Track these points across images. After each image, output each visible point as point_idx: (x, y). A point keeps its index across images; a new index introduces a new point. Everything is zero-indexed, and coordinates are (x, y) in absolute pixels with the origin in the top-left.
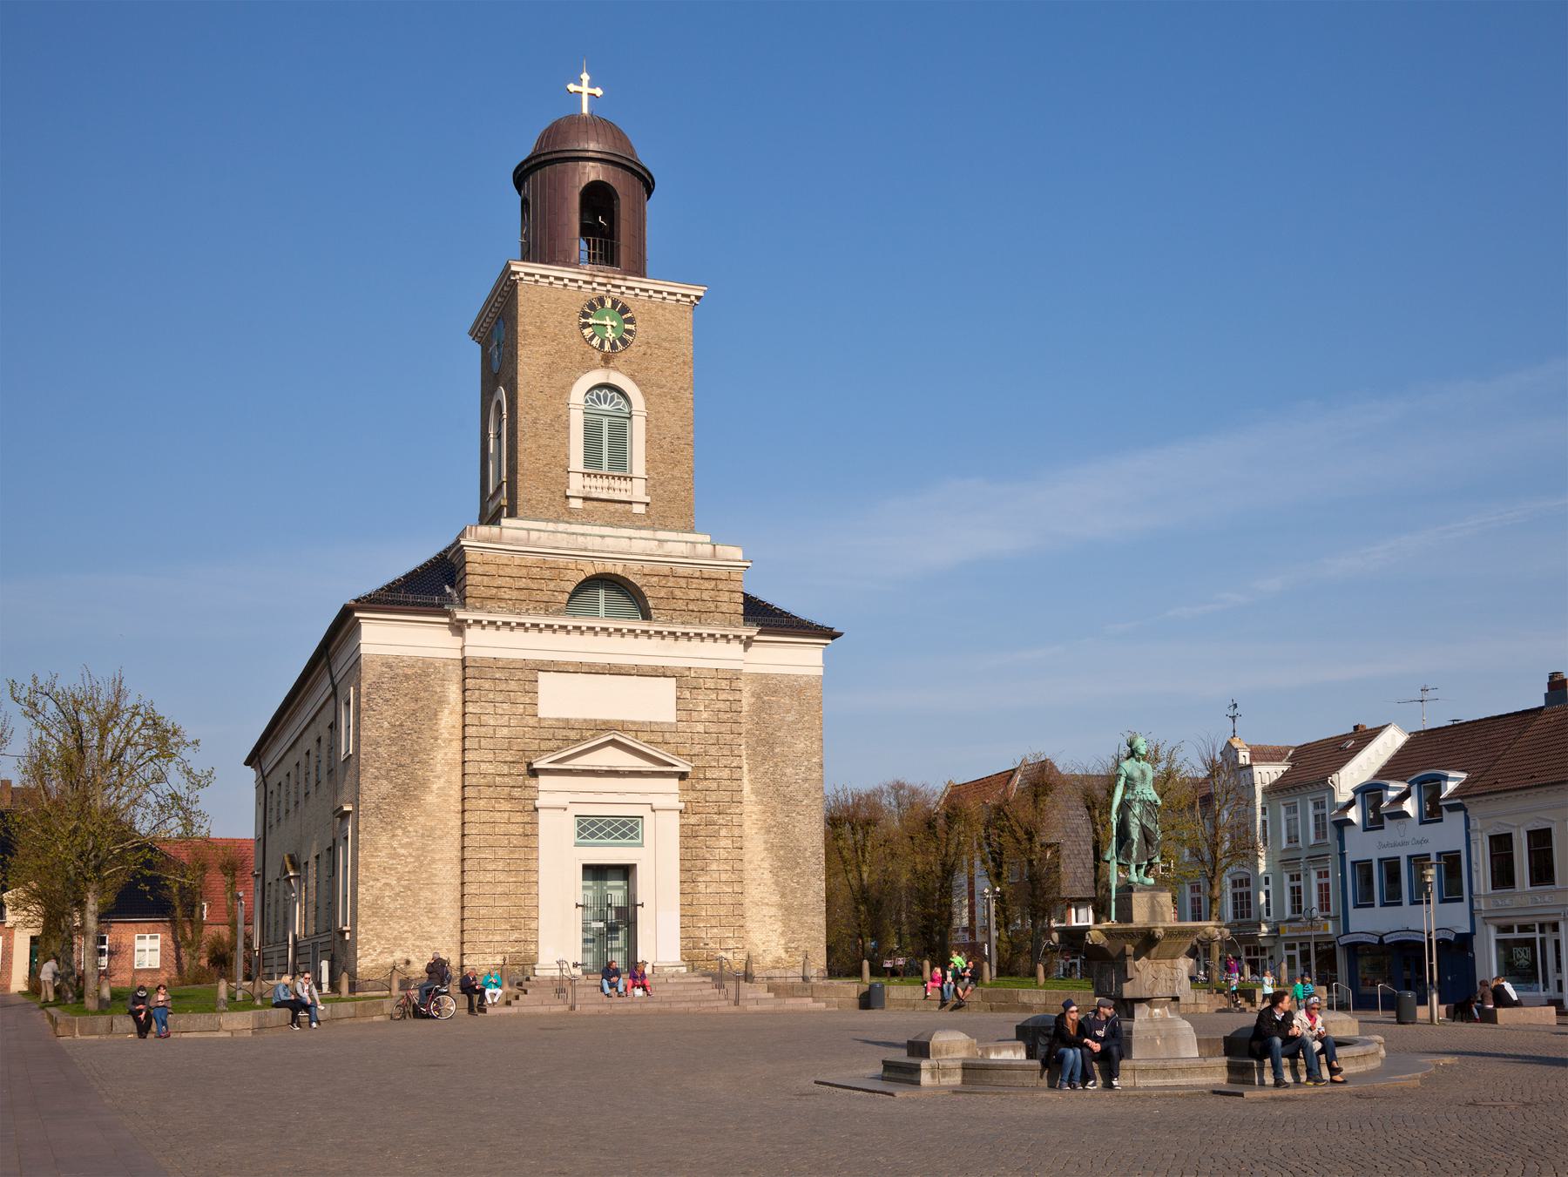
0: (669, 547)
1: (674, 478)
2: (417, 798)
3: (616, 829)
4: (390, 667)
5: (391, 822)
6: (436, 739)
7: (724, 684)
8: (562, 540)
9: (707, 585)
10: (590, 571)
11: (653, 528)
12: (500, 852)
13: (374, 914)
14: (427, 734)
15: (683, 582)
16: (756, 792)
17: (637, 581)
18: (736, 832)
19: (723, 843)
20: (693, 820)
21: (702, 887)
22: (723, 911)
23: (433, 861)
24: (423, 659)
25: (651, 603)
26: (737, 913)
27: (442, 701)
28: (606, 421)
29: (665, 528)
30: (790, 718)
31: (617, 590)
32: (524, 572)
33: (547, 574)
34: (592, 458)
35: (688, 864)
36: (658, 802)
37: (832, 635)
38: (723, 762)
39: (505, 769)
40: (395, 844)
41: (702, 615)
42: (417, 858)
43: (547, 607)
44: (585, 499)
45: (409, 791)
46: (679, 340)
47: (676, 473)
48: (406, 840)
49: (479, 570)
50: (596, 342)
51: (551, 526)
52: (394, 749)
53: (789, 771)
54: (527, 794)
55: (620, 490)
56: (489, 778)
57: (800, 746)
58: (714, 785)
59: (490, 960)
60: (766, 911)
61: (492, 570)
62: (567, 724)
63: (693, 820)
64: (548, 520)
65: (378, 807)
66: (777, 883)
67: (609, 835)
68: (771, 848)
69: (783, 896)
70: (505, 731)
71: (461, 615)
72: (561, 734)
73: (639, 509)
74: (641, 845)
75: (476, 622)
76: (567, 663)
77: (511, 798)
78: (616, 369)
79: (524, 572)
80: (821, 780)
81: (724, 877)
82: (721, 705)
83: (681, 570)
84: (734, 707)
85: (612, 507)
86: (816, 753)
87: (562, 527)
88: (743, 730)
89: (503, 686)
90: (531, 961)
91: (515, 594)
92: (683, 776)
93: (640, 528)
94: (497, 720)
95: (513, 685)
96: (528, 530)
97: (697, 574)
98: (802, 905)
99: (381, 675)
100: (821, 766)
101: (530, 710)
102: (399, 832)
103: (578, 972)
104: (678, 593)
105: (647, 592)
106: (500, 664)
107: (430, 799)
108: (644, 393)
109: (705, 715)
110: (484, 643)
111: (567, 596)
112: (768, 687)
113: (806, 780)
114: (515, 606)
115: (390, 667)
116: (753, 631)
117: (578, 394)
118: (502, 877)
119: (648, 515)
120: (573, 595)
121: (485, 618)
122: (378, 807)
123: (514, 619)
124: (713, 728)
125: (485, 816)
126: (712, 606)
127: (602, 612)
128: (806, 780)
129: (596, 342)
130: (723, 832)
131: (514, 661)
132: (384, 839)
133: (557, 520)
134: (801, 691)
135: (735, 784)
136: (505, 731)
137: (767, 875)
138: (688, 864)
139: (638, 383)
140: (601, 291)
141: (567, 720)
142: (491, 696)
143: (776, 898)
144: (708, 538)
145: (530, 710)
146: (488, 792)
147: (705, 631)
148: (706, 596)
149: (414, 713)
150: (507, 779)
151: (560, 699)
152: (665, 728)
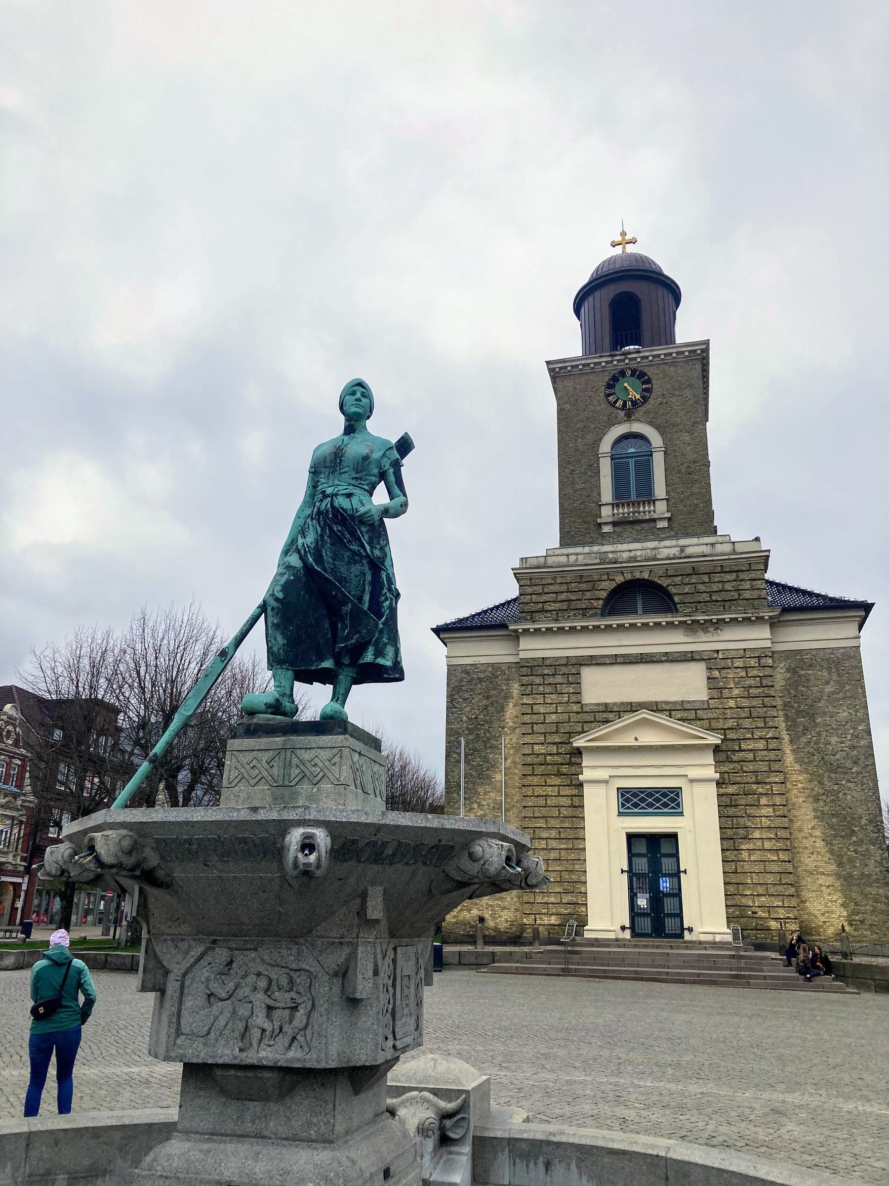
0: (689, 551)
1: (692, 494)
2: (489, 777)
3: (657, 800)
4: (468, 673)
6: (503, 728)
7: (753, 662)
9: (728, 577)
10: (620, 579)
11: (676, 537)
12: (553, 823)
14: (496, 725)
15: (706, 578)
16: (798, 761)
17: (664, 582)
18: (778, 800)
19: (765, 811)
20: (731, 789)
21: (745, 855)
22: (770, 879)
25: (676, 599)
26: (791, 884)
27: (507, 697)
28: (632, 462)
29: (686, 535)
30: (828, 689)
32: (564, 588)
33: (584, 586)
35: (729, 833)
36: (693, 773)
38: (758, 734)
39: (554, 749)
43: (584, 612)
50: (619, 404)
51: (587, 549)
52: (471, 737)
53: (834, 740)
54: (573, 769)
55: (645, 511)
57: (844, 715)
58: (750, 756)
59: (546, 920)
60: (822, 880)
61: (539, 589)
62: (607, 708)
63: (731, 789)
64: (583, 544)
66: (831, 852)
67: (650, 805)
68: (821, 816)
69: (840, 864)
73: (665, 524)
74: (681, 814)
75: (524, 630)
77: (559, 774)
79: (564, 588)
81: (767, 845)
82: (751, 682)
83: (702, 570)
84: (765, 682)
87: (596, 548)
88: (779, 702)
89: (551, 680)
90: (583, 922)
91: (557, 606)
92: (717, 749)
94: (549, 709)
95: (559, 679)
96: (568, 555)
97: (719, 569)
98: (863, 874)
99: (461, 680)
101: (573, 698)
102: (475, 806)
103: (627, 935)
104: (701, 588)
105: (673, 590)
106: (548, 662)
107: (499, 777)
109: (736, 692)
111: (601, 602)
113: (853, 748)
114: (557, 616)
115: (468, 673)
117: (606, 446)
118: (553, 844)
119: (670, 527)
120: (607, 600)
123: (554, 625)
124: (745, 703)
125: (539, 791)
126: (735, 595)
127: (640, 611)
128: (853, 748)
129: (619, 404)
130: (764, 801)
133: (593, 543)
134: (838, 663)
135: (772, 755)
136: (554, 717)
137: (820, 844)
138: (729, 833)
139: (658, 428)
140: (622, 366)
141: (606, 705)
142: (541, 688)
143: (833, 867)
145: (573, 698)
146: (540, 770)
148: (728, 586)
149: (486, 708)
150: (556, 758)
152: (698, 706)
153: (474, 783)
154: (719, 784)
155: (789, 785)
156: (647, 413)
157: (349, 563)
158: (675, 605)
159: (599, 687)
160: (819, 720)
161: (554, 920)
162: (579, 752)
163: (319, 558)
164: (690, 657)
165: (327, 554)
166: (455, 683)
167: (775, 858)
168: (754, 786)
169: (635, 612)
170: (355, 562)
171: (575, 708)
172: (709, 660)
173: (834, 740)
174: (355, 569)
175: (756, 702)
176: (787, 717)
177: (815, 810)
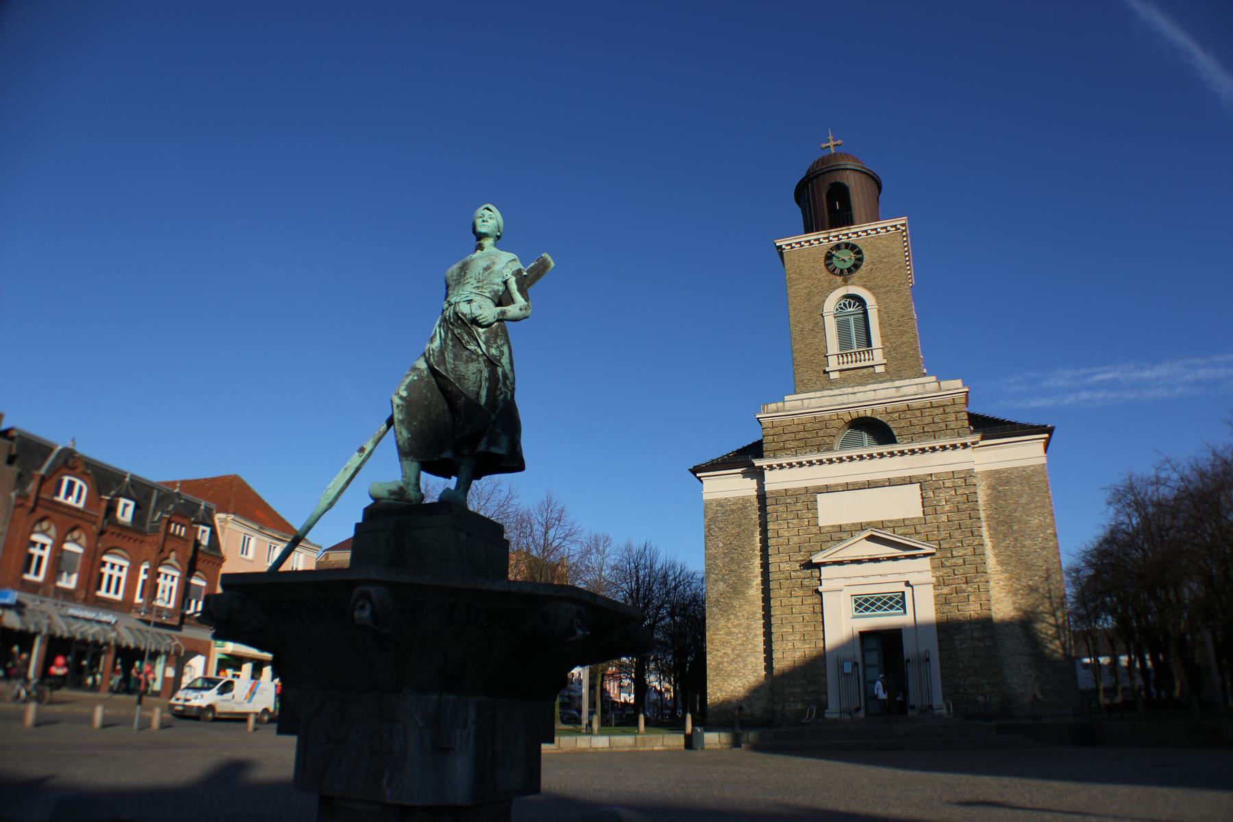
0: (904, 391)
1: (903, 343)
2: (743, 593)
5: (726, 610)
8: (826, 402)
9: (937, 411)
13: (718, 674)
16: (1000, 563)
20: (946, 590)
23: (756, 635)
24: (743, 498)
25: (895, 432)
29: (901, 378)
30: (1023, 501)
31: (876, 429)
34: (844, 342)
37: (1050, 431)
40: (730, 625)
41: (934, 435)
42: (745, 634)
44: (840, 370)
45: (738, 589)
46: (894, 255)
47: (904, 339)
48: (736, 622)
49: (771, 432)
51: (818, 394)
53: (1028, 543)
56: (787, 574)
57: (1035, 522)
62: (840, 528)
63: (946, 590)
65: (717, 600)
67: (879, 608)
70: (796, 539)
71: (758, 463)
72: (835, 536)
76: (837, 485)
78: (853, 284)
80: (1057, 547)
81: (976, 634)
82: (959, 498)
83: (915, 404)
85: (860, 372)
86: (1049, 526)
87: (826, 393)
90: (823, 706)
91: (794, 444)
93: (881, 382)
100: (1055, 535)
102: (732, 617)
104: (914, 421)
105: (891, 425)
108: (874, 294)
109: (947, 508)
110: (776, 481)
112: (1001, 480)
113: (1043, 549)
116: (977, 437)
119: (887, 372)
121: (774, 462)
122: (717, 600)
124: (955, 517)
131: (799, 489)
132: (722, 622)
133: (823, 389)
139: (869, 289)
144: (933, 378)
146: (786, 584)
147: (937, 444)
148: (936, 420)
149: (739, 534)
151: (832, 511)
153: (730, 598)
154: (935, 587)
155: (992, 584)
156: (861, 277)
157: (467, 362)
158: (894, 437)
159: (833, 511)
160: (1015, 528)
161: (799, 706)
162: (818, 566)
163: (442, 360)
164: (909, 481)
165: (449, 356)
166: (710, 515)
167: (982, 645)
168: (964, 586)
169: (862, 445)
170: (473, 360)
171: (814, 530)
172: (924, 483)
173: (1028, 543)
174: (473, 367)
175: (964, 516)
176: (990, 527)
177: (1014, 603)
